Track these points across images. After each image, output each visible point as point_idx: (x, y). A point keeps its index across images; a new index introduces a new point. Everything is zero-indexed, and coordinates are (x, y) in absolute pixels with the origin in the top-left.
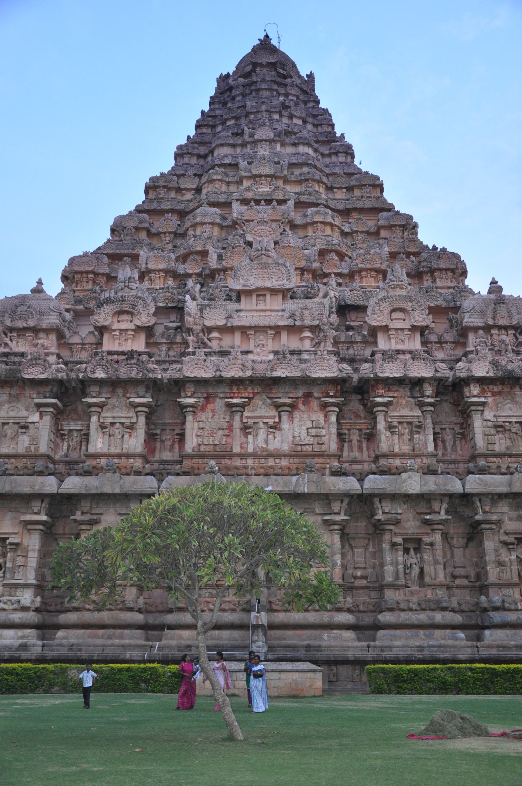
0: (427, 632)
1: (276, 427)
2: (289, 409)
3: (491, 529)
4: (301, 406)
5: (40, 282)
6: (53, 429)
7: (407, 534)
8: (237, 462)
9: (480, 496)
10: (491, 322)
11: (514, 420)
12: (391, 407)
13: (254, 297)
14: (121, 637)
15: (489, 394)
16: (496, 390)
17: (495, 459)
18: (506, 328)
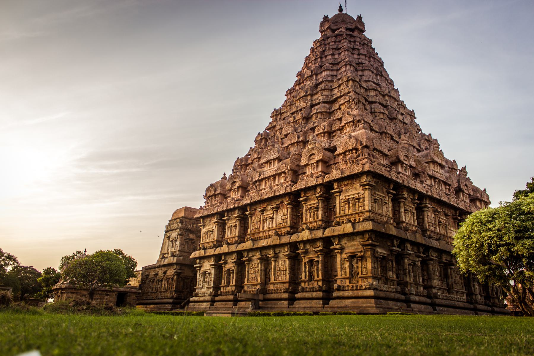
0: (309, 301)
1: (272, 218)
2: (276, 209)
3: (338, 252)
4: (281, 208)
5: (225, 174)
6: (221, 230)
7: (309, 258)
8: (261, 235)
9: (334, 237)
10: (345, 149)
11: (353, 197)
12: (308, 201)
13: (269, 164)
14: (228, 305)
15: (343, 186)
16: (346, 183)
17: (343, 218)
18: (351, 150)
